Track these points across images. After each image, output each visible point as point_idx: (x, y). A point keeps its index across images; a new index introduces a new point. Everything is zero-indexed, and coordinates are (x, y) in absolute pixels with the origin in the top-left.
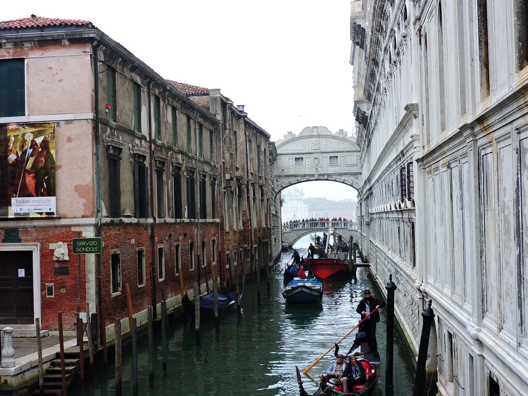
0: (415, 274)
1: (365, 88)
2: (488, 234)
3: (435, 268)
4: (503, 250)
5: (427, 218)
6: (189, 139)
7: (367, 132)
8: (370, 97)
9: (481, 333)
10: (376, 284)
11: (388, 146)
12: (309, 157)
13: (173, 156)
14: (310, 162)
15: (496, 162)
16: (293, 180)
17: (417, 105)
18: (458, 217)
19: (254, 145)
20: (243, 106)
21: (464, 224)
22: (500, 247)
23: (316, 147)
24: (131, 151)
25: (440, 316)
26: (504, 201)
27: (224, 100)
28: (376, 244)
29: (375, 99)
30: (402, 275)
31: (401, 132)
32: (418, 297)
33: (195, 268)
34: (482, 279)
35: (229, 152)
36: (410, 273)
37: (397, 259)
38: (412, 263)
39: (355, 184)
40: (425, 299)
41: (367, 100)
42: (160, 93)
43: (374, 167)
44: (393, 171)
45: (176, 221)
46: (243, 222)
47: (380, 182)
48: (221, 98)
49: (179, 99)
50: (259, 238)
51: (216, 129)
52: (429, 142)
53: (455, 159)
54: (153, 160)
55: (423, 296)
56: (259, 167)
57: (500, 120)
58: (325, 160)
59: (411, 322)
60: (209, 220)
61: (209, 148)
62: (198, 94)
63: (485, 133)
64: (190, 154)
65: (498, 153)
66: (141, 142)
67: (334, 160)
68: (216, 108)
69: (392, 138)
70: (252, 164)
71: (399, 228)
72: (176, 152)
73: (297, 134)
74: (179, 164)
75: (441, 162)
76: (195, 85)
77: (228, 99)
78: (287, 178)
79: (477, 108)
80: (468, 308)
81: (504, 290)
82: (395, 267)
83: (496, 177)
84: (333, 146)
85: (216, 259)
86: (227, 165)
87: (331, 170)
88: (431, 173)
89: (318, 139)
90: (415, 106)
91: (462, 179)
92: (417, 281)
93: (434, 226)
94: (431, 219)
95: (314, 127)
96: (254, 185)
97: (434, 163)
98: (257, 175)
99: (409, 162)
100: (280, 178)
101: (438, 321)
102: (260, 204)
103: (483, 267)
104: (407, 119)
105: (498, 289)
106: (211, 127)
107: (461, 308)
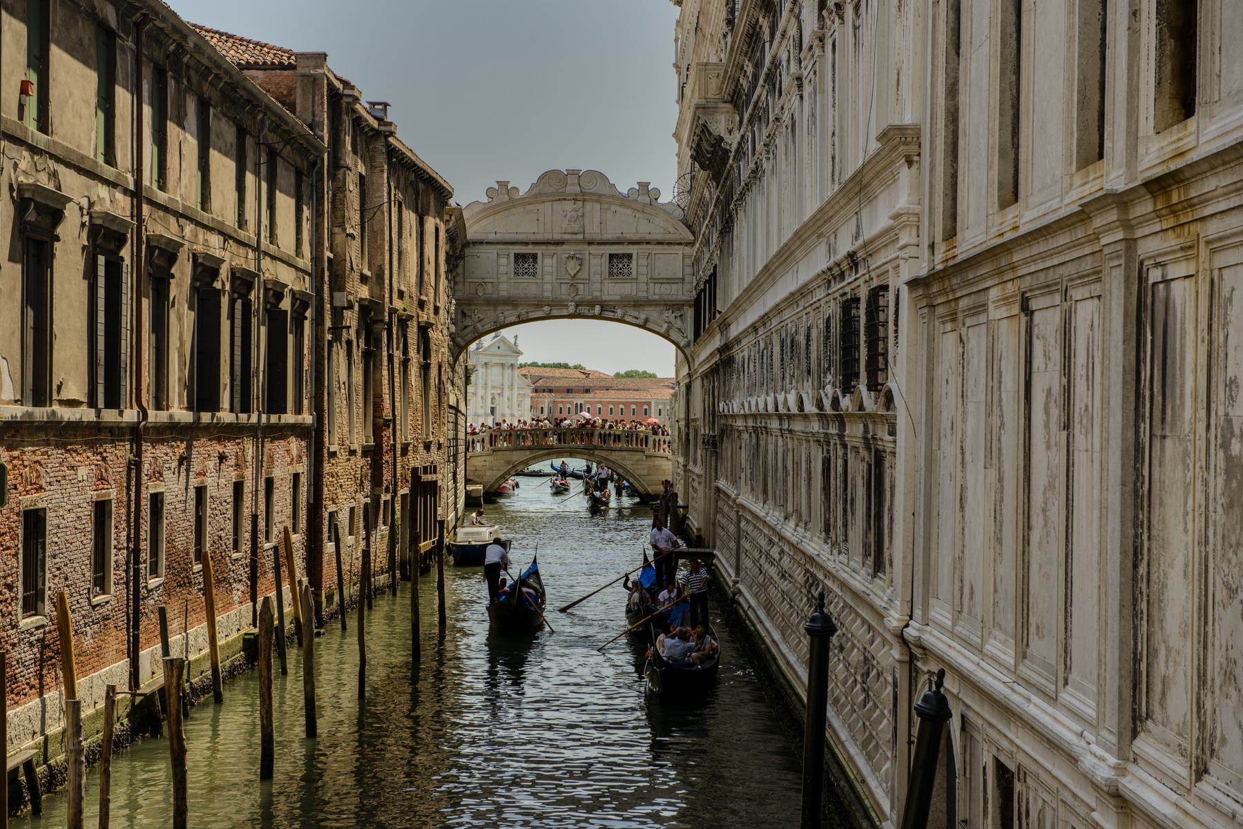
0: (882, 594)
2: (1161, 504)
3: (956, 582)
4: (1219, 553)
5: (935, 442)
8: (739, 97)
9: (1129, 778)
10: (736, 608)
11: (804, 237)
13: (196, 236)
14: (555, 266)
15: (1207, 304)
17: (917, 130)
18: (1048, 448)
20: (386, 105)
21: (1071, 469)
22: (1207, 543)
23: (576, 227)
25: (971, 715)
26: (1226, 415)
28: (741, 500)
29: (757, 103)
32: (897, 656)
34: (1135, 628)
36: (865, 589)
37: (817, 548)
38: (870, 561)
40: (919, 664)
41: (729, 106)
42: (168, 57)
44: (814, 306)
47: (761, 331)
48: (328, 79)
50: (415, 470)
51: (314, 164)
52: (951, 234)
53: (1048, 286)
55: (912, 657)
57: (1233, 187)
58: (597, 261)
59: (861, 723)
60: (289, 418)
62: (265, 63)
63: (1171, 222)
65: (1212, 281)
67: (620, 266)
68: (313, 106)
71: (827, 462)
72: (205, 227)
73: (524, 189)
75: (994, 293)
77: (346, 84)
79: (1141, 150)
80: (1077, 704)
81: (1217, 664)
82: (808, 566)
83: (1203, 349)
84: (620, 224)
87: (614, 290)
88: (954, 320)
90: (909, 132)
91: (1070, 346)
92: (892, 612)
93: (959, 467)
94: (948, 449)
95: (574, 173)
97: (970, 294)
98: (415, 299)
99: (875, 284)
100: (473, 307)
101: (963, 729)
103: (1141, 593)
104: (879, 167)
105: (1195, 659)
106: (299, 159)
107: (1053, 699)
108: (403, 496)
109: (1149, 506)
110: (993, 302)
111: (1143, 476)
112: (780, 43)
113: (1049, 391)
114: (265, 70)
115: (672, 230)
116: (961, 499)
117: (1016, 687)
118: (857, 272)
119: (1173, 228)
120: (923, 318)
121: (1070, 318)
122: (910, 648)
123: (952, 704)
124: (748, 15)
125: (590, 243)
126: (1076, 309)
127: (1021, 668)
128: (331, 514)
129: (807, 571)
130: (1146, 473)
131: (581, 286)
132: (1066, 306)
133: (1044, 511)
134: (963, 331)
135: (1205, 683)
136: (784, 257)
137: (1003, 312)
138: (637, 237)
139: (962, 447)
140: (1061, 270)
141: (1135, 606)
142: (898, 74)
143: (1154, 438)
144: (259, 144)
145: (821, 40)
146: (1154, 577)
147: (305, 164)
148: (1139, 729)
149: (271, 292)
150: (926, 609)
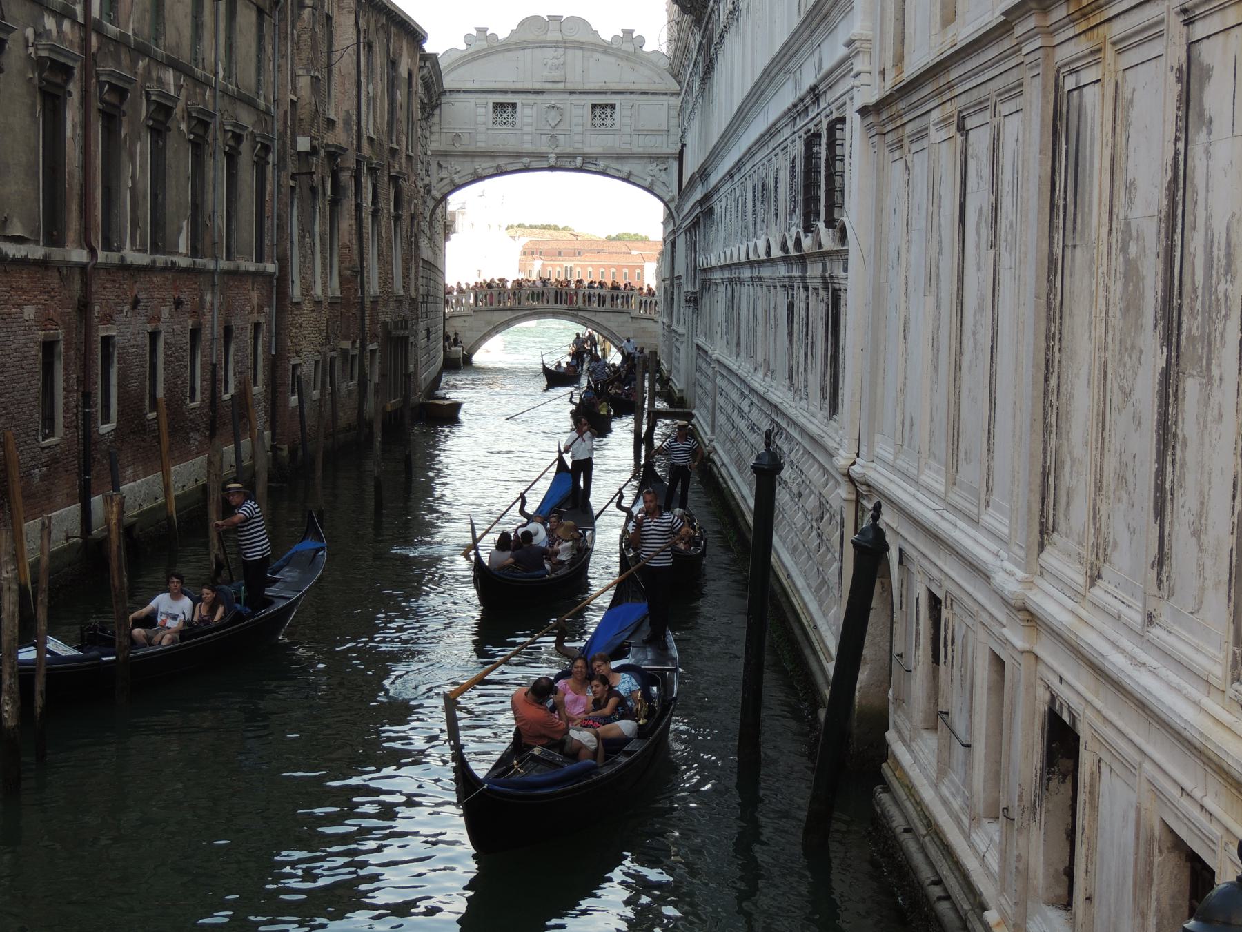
0: (834, 435)
2: (1071, 315)
4: (1117, 358)
5: (883, 275)
6: (197, 27)
7: (703, 37)
9: (1035, 590)
10: (710, 467)
11: (772, 75)
13: (150, 73)
15: (1112, 107)
16: (484, 165)
18: (979, 269)
19: (379, 60)
21: (997, 288)
22: (1106, 349)
23: (556, 75)
24: (31, 50)
25: (907, 548)
26: (1126, 218)
30: (792, 438)
31: (813, 32)
32: (844, 495)
33: (203, 401)
35: (308, 71)
40: (865, 502)
43: (723, 137)
45: (154, 262)
46: (341, 276)
47: (737, 178)
50: (385, 324)
52: (899, 59)
53: (981, 103)
55: (858, 495)
56: (390, 123)
58: (579, 111)
61: (254, 60)
63: (1082, 26)
64: (199, 71)
65: (1117, 83)
66: (59, 26)
67: (603, 116)
70: (371, 113)
71: (791, 306)
72: (158, 63)
73: (503, 33)
74: (168, 97)
75: (935, 115)
78: (469, 159)
80: (996, 524)
82: (773, 416)
83: (1107, 152)
85: (261, 377)
86: (303, 111)
87: (595, 143)
88: (901, 147)
89: (561, 51)
91: (998, 163)
92: (841, 452)
93: (903, 298)
95: (553, 18)
96: (376, 174)
99: (834, 116)
100: (449, 159)
101: (901, 562)
102: (389, 228)
103: (1051, 406)
105: (1093, 465)
107: (975, 522)
108: (373, 351)
109: (1061, 318)
110: (934, 125)
111: (1056, 288)
113: (981, 210)
115: (657, 79)
116: (904, 330)
117: (946, 514)
118: (819, 105)
119: (1084, 32)
120: (874, 147)
121: (999, 134)
123: (889, 538)
125: (572, 93)
127: (950, 494)
128: (295, 367)
129: (773, 421)
130: (1058, 285)
131: (561, 138)
133: (974, 333)
134: (909, 157)
135: (1100, 489)
136: (756, 97)
137: (943, 135)
139: (906, 277)
140: (991, 85)
141: (1045, 419)
143: (1066, 249)
146: (1063, 389)
148: (1046, 542)
149: (230, 134)
150: (871, 446)
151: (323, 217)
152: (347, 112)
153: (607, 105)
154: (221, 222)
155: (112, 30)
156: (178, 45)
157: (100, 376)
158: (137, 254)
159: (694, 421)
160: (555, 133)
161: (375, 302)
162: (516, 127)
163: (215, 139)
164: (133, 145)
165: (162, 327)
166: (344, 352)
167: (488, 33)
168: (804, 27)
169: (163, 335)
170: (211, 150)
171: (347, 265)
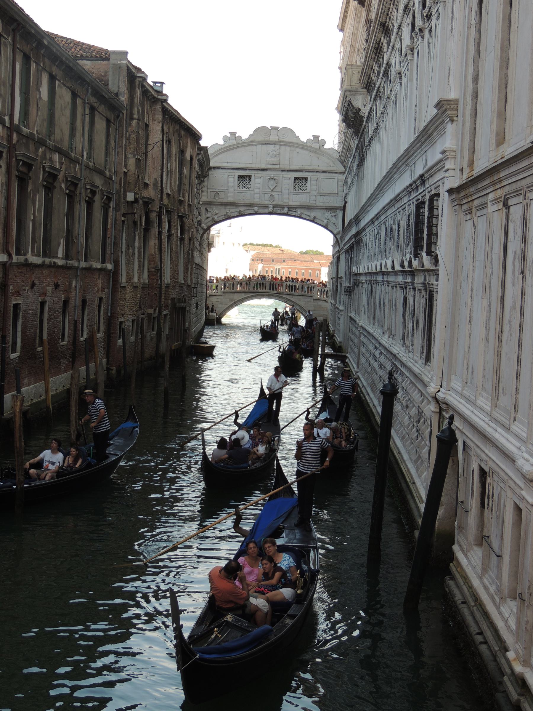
0: (427, 374)
1: (363, 70)
6: (73, 129)
7: (359, 142)
8: (370, 85)
11: (398, 167)
12: (260, 175)
13: (45, 155)
17: (456, 102)
18: (514, 285)
19: (174, 150)
20: (162, 83)
21: (524, 297)
23: (274, 160)
25: (468, 441)
27: (133, 70)
29: (379, 88)
31: (422, 144)
32: (433, 409)
33: (69, 341)
35: (134, 156)
36: (420, 372)
37: (398, 349)
39: (332, 225)
40: (444, 413)
41: (364, 90)
42: (32, 50)
43: (369, 200)
44: (403, 207)
45: (44, 262)
46: (149, 272)
47: (376, 223)
48: (128, 67)
49: (62, 63)
50: (173, 300)
51: (118, 116)
52: (471, 163)
53: (517, 191)
54: (14, 159)
55: (441, 409)
56: (180, 185)
61: (104, 148)
62: (92, 56)
64: (73, 154)
67: (300, 184)
69: (405, 154)
70: (169, 180)
71: (405, 299)
74: (55, 169)
75: (491, 196)
76: (87, 42)
77: (139, 70)
78: (223, 207)
80: (519, 431)
82: (393, 361)
87: (295, 200)
88: (471, 213)
89: (277, 147)
90: (452, 103)
92: (432, 384)
93: (470, 299)
95: (273, 128)
96: (171, 214)
99: (433, 192)
100: (212, 206)
101: (464, 449)
102: (177, 245)
104: (437, 124)
106: (109, 113)
107: (507, 429)
108: (165, 315)
110: (491, 202)
112: (391, 52)
113: (515, 252)
114: (92, 60)
115: (332, 164)
116: (470, 317)
117: (491, 423)
118: (424, 186)
121: (527, 210)
122: (440, 404)
123: (458, 435)
124: (375, 36)
126: (530, 204)
127: (494, 412)
128: (121, 323)
129: (393, 363)
131: (276, 196)
132: (525, 202)
133: (510, 322)
134: (475, 219)
137: (495, 207)
138: (311, 168)
139: (472, 287)
140: (524, 182)
142: (449, 69)
144: (85, 103)
145: (412, 50)
147: (113, 116)
149: (89, 190)
150: (449, 381)
151: (140, 238)
152: (156, 179)
153: (303, 178)
154: (82, 240)
155: (25, 130)
156: (62, 140)
157: (11, 326)
158: (35, 258)
159: (347, 360)
160: (273, 193)
161: (167, 287)
162: (251, 189)
163: (81, 193)
164: (35, 196)
165: (47, 299)
166: (149, 315)
167: (237, 135)
168: (417, 141)
169: (48, 303)
170: (78, 199)
171: (152, 265)
